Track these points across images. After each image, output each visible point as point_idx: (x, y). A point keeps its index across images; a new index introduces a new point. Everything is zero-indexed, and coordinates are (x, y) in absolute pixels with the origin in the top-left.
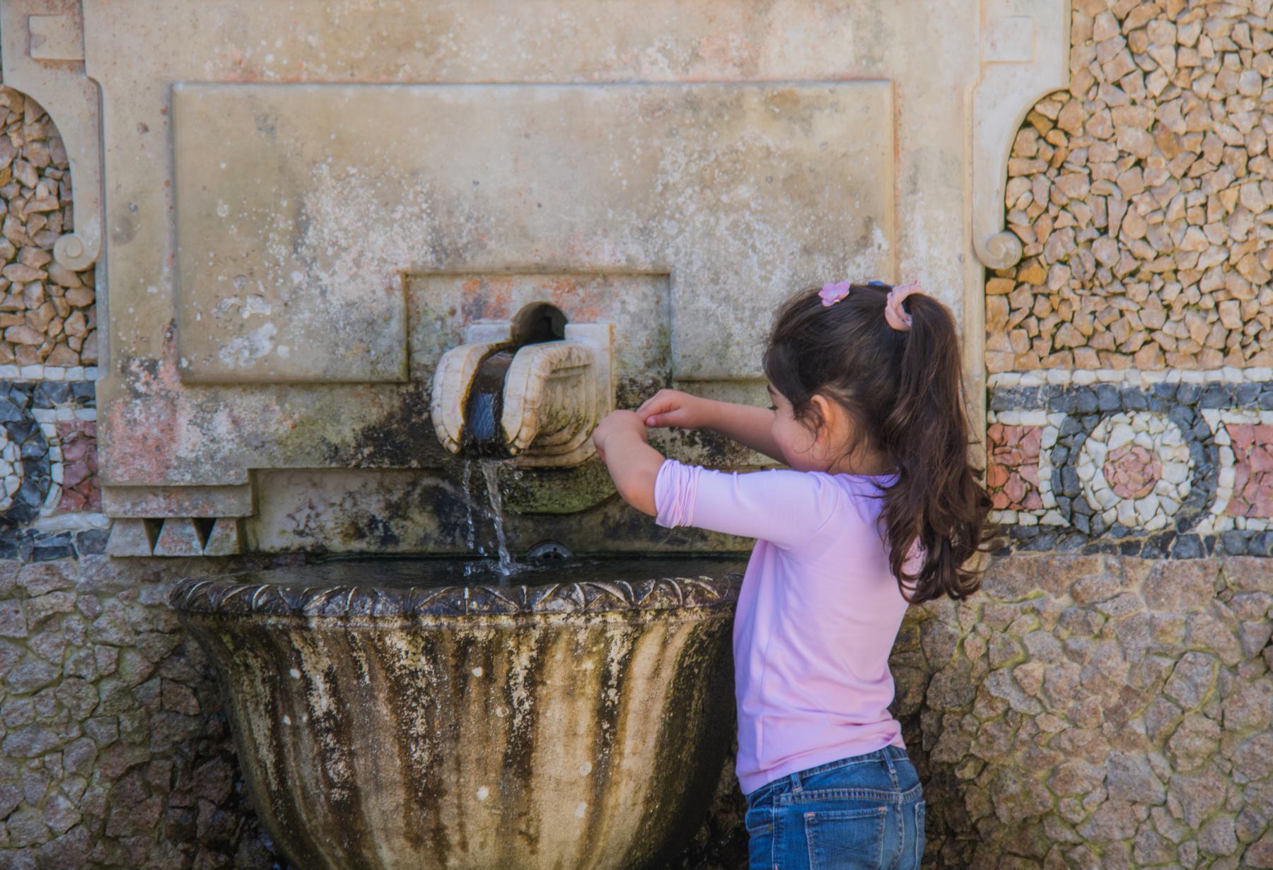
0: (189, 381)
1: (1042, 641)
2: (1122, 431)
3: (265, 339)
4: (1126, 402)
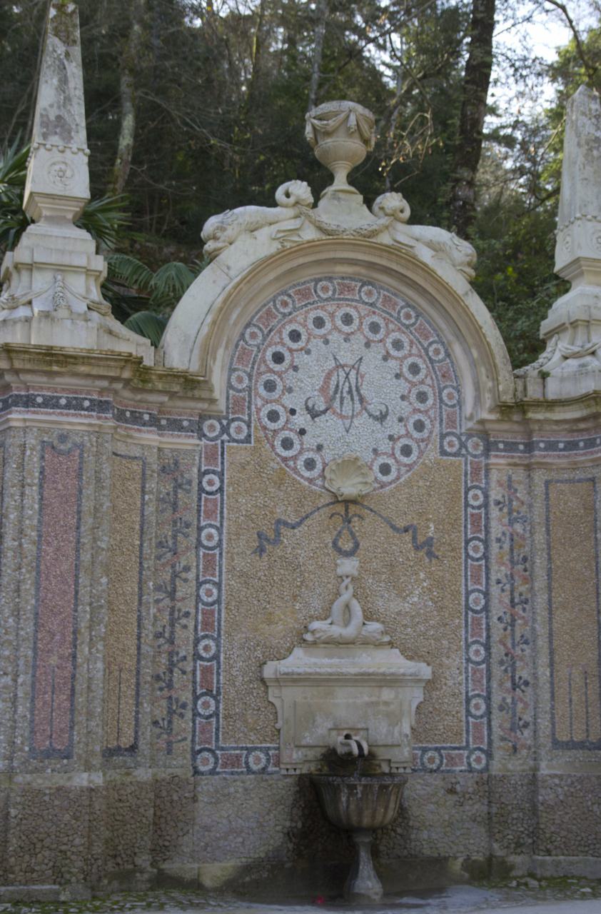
0: (296, 746)
1: (419, 787)
2: (430, 754)
3: (308, 740)
4: (430, 749)
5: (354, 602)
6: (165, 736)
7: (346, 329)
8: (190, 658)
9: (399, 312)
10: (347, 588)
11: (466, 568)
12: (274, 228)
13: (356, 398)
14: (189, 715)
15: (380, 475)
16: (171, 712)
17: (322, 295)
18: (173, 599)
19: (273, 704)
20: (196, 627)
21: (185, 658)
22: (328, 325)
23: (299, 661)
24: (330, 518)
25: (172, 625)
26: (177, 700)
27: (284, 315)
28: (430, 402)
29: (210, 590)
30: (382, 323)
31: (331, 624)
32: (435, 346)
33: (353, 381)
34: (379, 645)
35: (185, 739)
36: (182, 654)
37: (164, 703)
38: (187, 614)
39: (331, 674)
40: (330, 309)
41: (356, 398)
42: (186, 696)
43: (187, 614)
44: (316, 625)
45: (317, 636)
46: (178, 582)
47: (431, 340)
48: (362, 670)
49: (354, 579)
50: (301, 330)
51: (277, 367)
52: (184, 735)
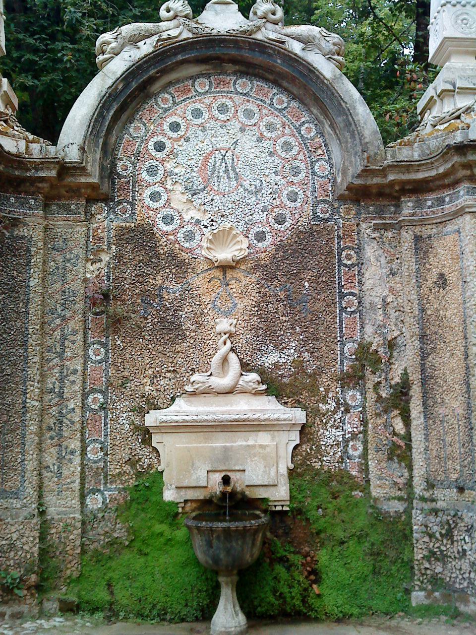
5: (232, 356)
6: (56, 479)
7: (223, 117)
8: (78, 411)
9: (272, 99)
10: (225, 343)
11: (341, 321)
12: (156, 38)
13: (232, 175)
14: (77, 460)
15: (255, 242)
16: (60, 458)
17: (199, 90)
18: (62, 359)
19: (157, 452)
20: (84, 382)
21: (73, 409)
22: (206, 116)
23: (183, 409)
24: (209, 282)
25: (61, 380)
26: (66, 448)
27: (166, 110)
28: (302, 175)
29: (99, 350)
30: (256, 110)
31: (211, 375)
32: (306, 125)
33: (229, 162)
34: (257, 393)
35: (74, 482)
36: (72, 406)
37: (54, 450)
38: (75, 372)
39: (206, 421)
40: (207, 101)
41: (232, 175)
42: (75, 444)
43: (75, 372)
44: (196, 377)
45: (196, 387)
46: (66, 343)
47: (303, 120)
48: (237, 417)
49: (231, 335)
50: (179, 120)
51: (159, 155)
52: (73, 479)
